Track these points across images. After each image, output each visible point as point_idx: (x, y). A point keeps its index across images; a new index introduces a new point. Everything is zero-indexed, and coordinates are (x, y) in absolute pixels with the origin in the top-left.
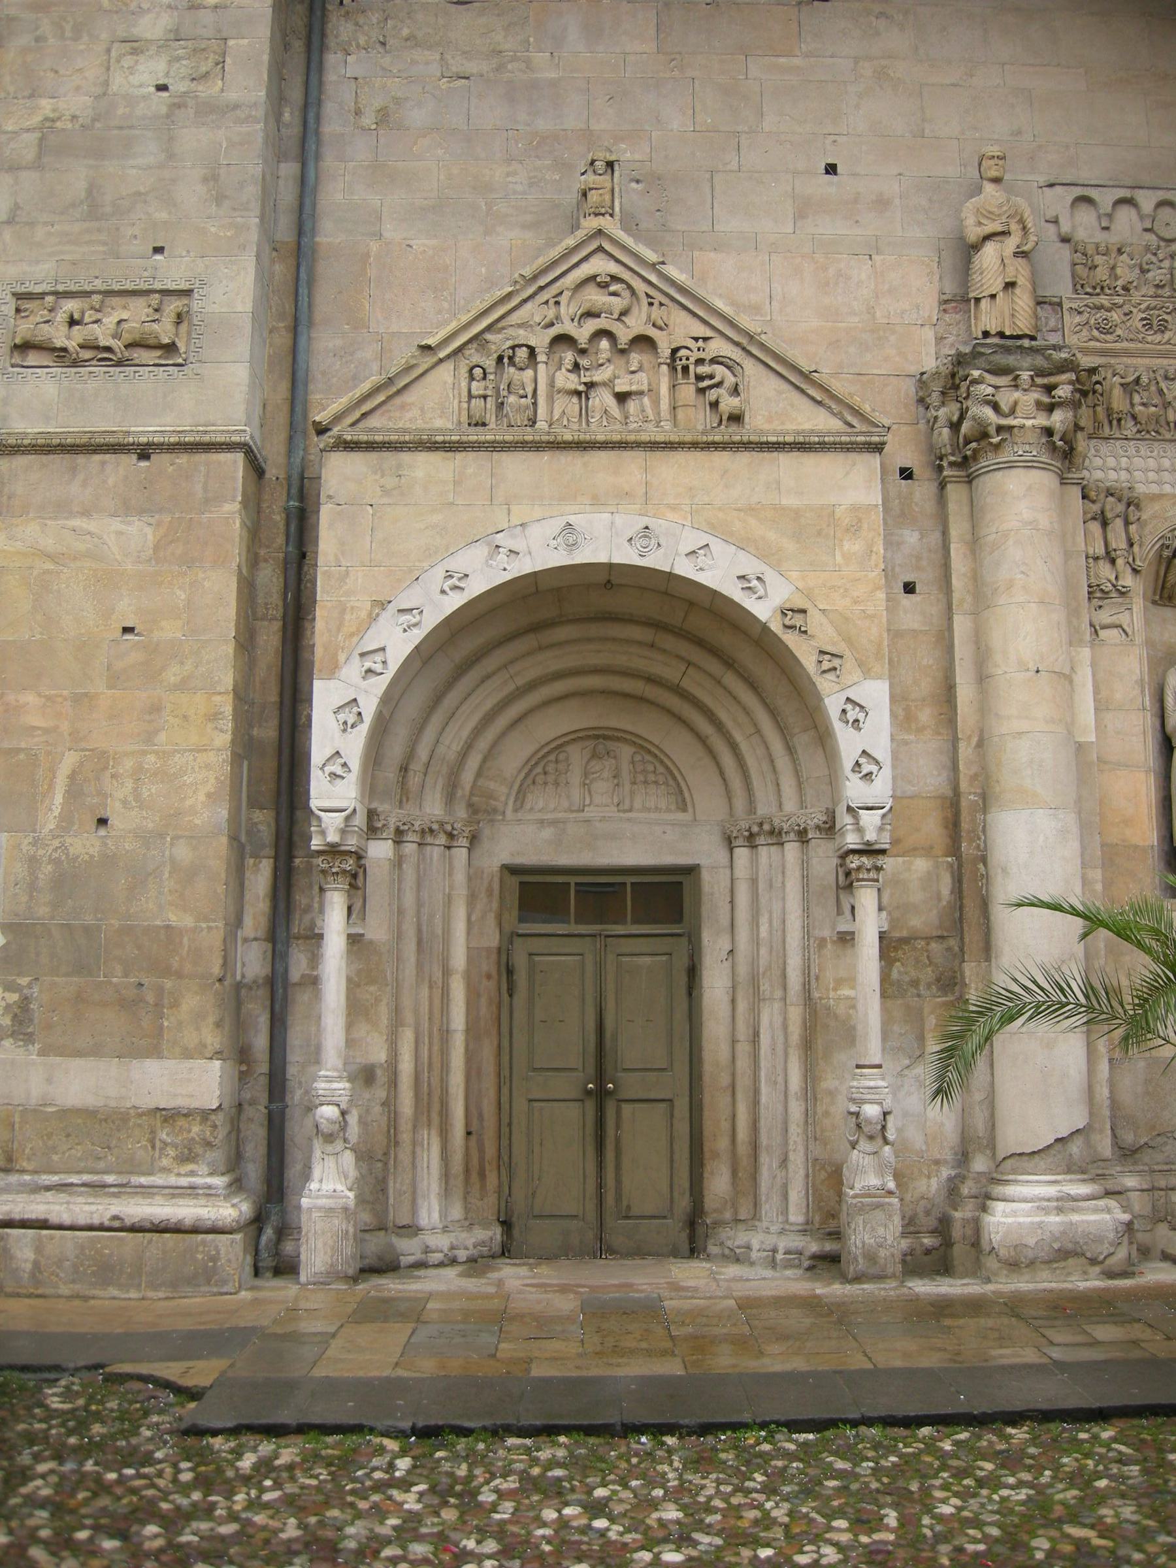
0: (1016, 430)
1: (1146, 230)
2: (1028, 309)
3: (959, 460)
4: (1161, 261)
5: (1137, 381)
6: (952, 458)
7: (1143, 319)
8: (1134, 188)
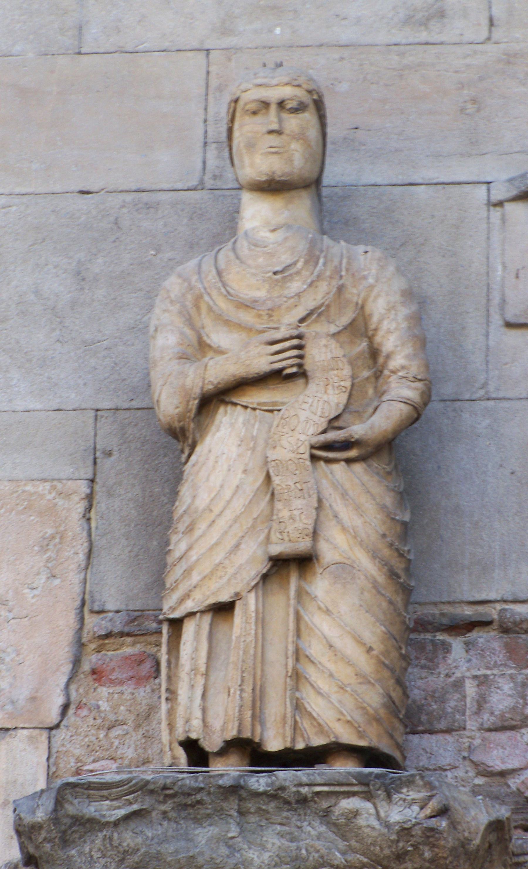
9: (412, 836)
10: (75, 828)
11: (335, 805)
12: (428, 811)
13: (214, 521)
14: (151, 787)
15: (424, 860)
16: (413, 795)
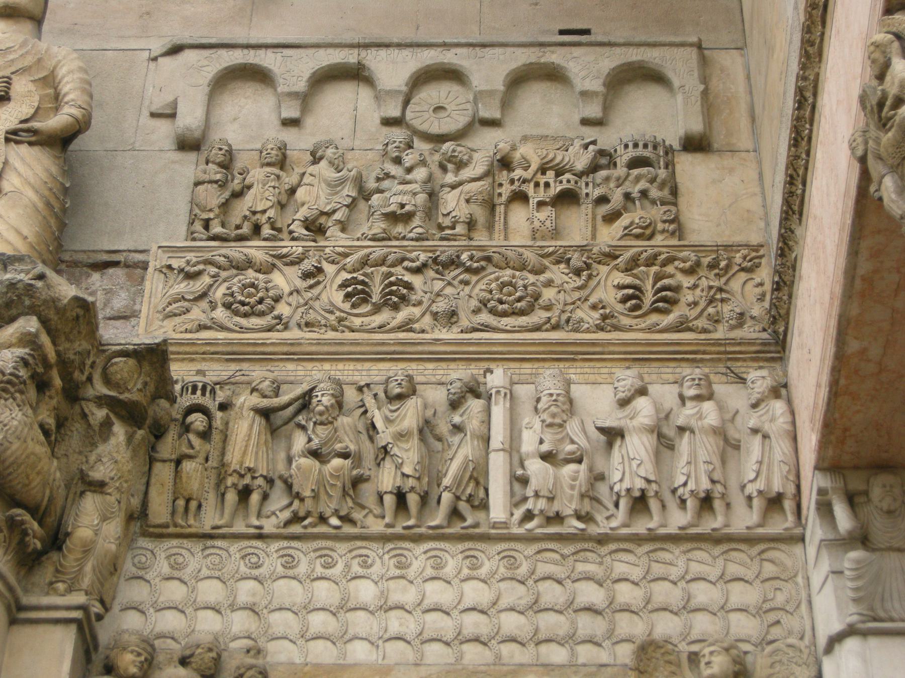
1: (388, 122)
4: (409, 170)
7: (344, 285)
8: (367, 46)
12: (30, 276)
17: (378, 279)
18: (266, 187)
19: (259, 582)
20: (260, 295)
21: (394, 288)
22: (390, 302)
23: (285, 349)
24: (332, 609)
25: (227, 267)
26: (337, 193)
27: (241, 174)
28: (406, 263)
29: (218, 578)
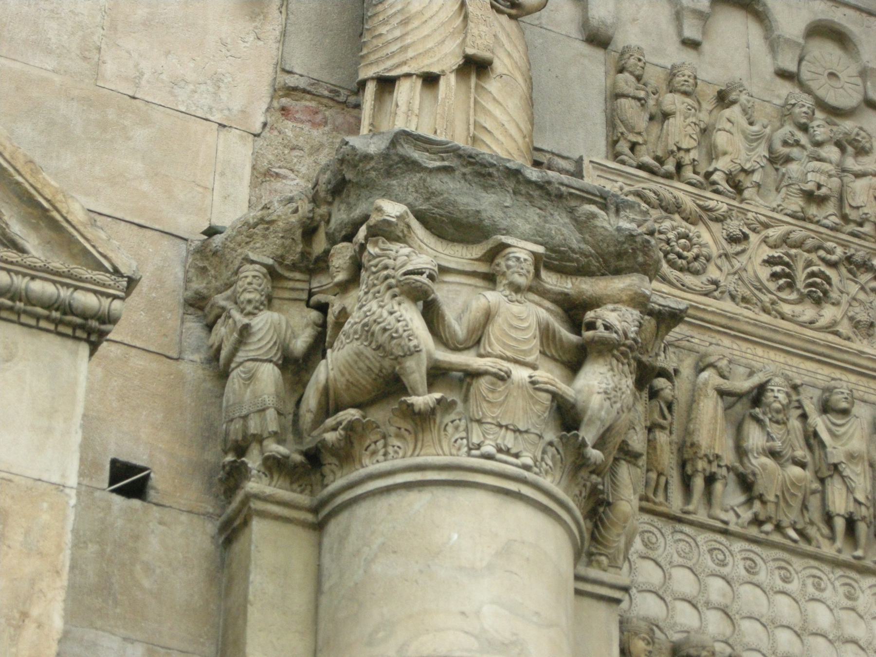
0: (483, 383)
1: (784, 75)
2: (513, 131)
3: (298, 458)
4: (818, 144)
5: (757, 396)
6: (274, 448)
7: (770, 262)
9: (635, 242)
10: (400, 165)
11: (580, 206)
13: (426, 21)
14: (461, 152)
15: (636, 262)
16: (632, 216)
17: (800, 264)
18: (688, 121)
19: (728, 583)
20: (695, 250)
21: (818, 280)
22: (815, 295)
23: (724, 321)
24: (797, 629)
25: (656, 206)
26: (753, 150)
27: (654, 94)
28: (822, 253)
29: (690, 569)
